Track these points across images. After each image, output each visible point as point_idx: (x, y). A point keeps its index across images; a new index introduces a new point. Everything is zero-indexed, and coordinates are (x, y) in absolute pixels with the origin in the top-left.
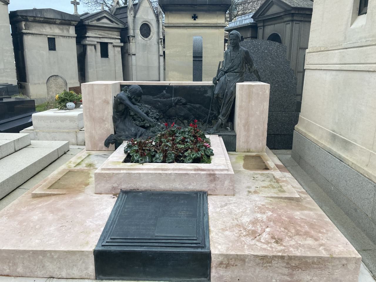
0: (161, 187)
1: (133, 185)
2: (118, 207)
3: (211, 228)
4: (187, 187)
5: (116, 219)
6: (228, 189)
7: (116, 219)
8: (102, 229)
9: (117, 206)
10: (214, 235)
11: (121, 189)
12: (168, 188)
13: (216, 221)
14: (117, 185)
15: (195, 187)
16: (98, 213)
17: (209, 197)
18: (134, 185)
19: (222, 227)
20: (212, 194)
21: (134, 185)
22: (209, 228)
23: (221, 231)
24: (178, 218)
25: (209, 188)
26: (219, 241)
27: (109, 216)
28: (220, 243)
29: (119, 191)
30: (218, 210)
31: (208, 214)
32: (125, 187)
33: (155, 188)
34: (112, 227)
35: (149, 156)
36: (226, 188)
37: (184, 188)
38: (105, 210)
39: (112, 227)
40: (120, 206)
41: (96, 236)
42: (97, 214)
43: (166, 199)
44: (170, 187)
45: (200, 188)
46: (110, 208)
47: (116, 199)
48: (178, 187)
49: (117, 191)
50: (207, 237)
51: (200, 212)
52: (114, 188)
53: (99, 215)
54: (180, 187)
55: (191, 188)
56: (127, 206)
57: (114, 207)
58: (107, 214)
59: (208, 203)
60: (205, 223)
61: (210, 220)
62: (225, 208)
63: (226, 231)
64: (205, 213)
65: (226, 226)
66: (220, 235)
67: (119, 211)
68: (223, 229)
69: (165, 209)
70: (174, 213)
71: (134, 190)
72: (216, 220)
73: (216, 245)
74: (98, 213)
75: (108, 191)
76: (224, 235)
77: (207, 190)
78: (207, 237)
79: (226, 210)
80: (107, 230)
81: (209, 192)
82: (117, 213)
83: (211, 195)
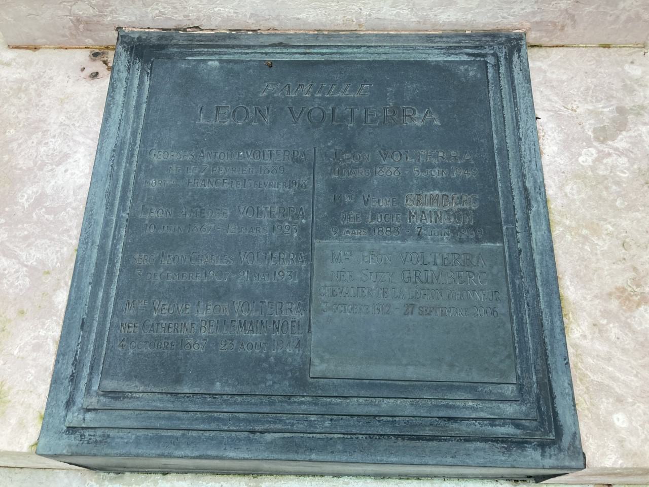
0: (303, 16)
1: (168, 11)
2: (118, 150)
3: (570, 290)
4: (431, 14)
5: (114, 246)
6: (629, 20)
7: (114, 246)
8: (61, 298)
9: (111, 146)
10: (585, 337)
11: (119, 29)
12: (340, 22)
13: (586, 238)
14: (91, 11)
15: (469, 17)
16: (31, 191)
17: (532, 53)
18: (175, 8)
19: (620, 281)
20: (545, 41)
21: (175, 8)
22: (561, 291)
23: (614, 305)
24: (410, 243)
25: (538, 19)
26: (613, 378)
27: (82, 208)
28: (619, 390)
29: (112, 37)
30: (587, 157)
31: (541, 187)
32: (134, 19)
33: (275, 24)
34: (101, 294)
35: (206, 153)
36: (623, 18)
37: (414, 19)
38: (62, 168)
39: (101, 294)
40: (123, 143)
41: (37, 347)
42: (26, 195)
43: (340, 101)
44: (349, 17)
45: (492, 21)
46: (82, 149)
47: (104, 83)
48: (387, 17)
49: (102, 34)
50: (560, 360)
51: (509, 190)
52: (83, 25)
53: (39, 201)
54: (398, 13)
55: (453, 19)
56: (157, 158)
57: (100, 151)
58: (75, 194)
59: (538, 113)
60: (537, 257)
61: (556, 231)
62: (621, 142)
63: (639, 305)
64: (529, 185)
65: (635, 269)
66: (613, 337)
67: (124, 182)
68: (624, 290)
69: (341, 173)
70: (384, 203)
71: (177, 30)
72: (585, 232)
73: (605, 405)
74: (31, 191)
75: (64, 36)
76: (634, 332)
77: (527, 25)
78: (560, 360)
79: (623, 160)
80: (82, 312)
81: (532, 37)
82: (115, 187)
83: (540, 46)
